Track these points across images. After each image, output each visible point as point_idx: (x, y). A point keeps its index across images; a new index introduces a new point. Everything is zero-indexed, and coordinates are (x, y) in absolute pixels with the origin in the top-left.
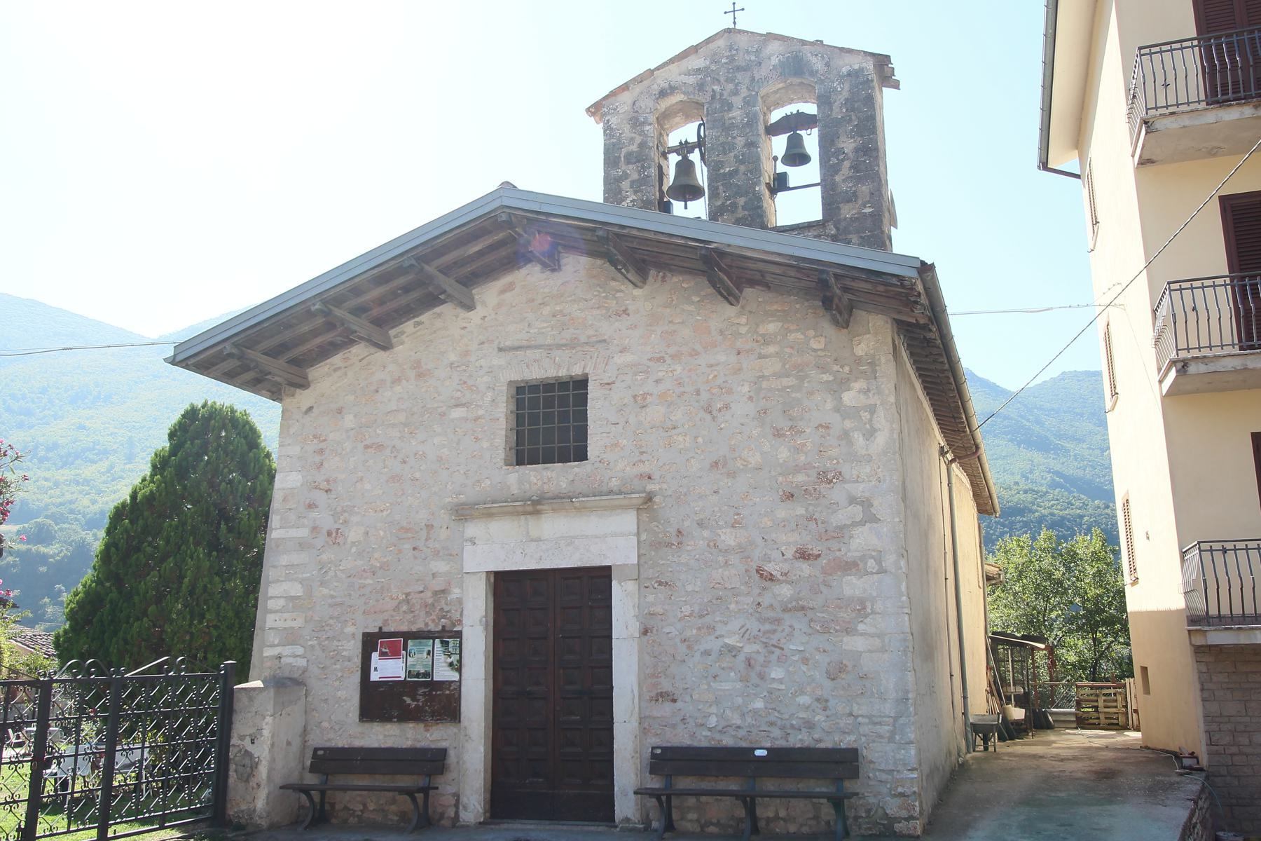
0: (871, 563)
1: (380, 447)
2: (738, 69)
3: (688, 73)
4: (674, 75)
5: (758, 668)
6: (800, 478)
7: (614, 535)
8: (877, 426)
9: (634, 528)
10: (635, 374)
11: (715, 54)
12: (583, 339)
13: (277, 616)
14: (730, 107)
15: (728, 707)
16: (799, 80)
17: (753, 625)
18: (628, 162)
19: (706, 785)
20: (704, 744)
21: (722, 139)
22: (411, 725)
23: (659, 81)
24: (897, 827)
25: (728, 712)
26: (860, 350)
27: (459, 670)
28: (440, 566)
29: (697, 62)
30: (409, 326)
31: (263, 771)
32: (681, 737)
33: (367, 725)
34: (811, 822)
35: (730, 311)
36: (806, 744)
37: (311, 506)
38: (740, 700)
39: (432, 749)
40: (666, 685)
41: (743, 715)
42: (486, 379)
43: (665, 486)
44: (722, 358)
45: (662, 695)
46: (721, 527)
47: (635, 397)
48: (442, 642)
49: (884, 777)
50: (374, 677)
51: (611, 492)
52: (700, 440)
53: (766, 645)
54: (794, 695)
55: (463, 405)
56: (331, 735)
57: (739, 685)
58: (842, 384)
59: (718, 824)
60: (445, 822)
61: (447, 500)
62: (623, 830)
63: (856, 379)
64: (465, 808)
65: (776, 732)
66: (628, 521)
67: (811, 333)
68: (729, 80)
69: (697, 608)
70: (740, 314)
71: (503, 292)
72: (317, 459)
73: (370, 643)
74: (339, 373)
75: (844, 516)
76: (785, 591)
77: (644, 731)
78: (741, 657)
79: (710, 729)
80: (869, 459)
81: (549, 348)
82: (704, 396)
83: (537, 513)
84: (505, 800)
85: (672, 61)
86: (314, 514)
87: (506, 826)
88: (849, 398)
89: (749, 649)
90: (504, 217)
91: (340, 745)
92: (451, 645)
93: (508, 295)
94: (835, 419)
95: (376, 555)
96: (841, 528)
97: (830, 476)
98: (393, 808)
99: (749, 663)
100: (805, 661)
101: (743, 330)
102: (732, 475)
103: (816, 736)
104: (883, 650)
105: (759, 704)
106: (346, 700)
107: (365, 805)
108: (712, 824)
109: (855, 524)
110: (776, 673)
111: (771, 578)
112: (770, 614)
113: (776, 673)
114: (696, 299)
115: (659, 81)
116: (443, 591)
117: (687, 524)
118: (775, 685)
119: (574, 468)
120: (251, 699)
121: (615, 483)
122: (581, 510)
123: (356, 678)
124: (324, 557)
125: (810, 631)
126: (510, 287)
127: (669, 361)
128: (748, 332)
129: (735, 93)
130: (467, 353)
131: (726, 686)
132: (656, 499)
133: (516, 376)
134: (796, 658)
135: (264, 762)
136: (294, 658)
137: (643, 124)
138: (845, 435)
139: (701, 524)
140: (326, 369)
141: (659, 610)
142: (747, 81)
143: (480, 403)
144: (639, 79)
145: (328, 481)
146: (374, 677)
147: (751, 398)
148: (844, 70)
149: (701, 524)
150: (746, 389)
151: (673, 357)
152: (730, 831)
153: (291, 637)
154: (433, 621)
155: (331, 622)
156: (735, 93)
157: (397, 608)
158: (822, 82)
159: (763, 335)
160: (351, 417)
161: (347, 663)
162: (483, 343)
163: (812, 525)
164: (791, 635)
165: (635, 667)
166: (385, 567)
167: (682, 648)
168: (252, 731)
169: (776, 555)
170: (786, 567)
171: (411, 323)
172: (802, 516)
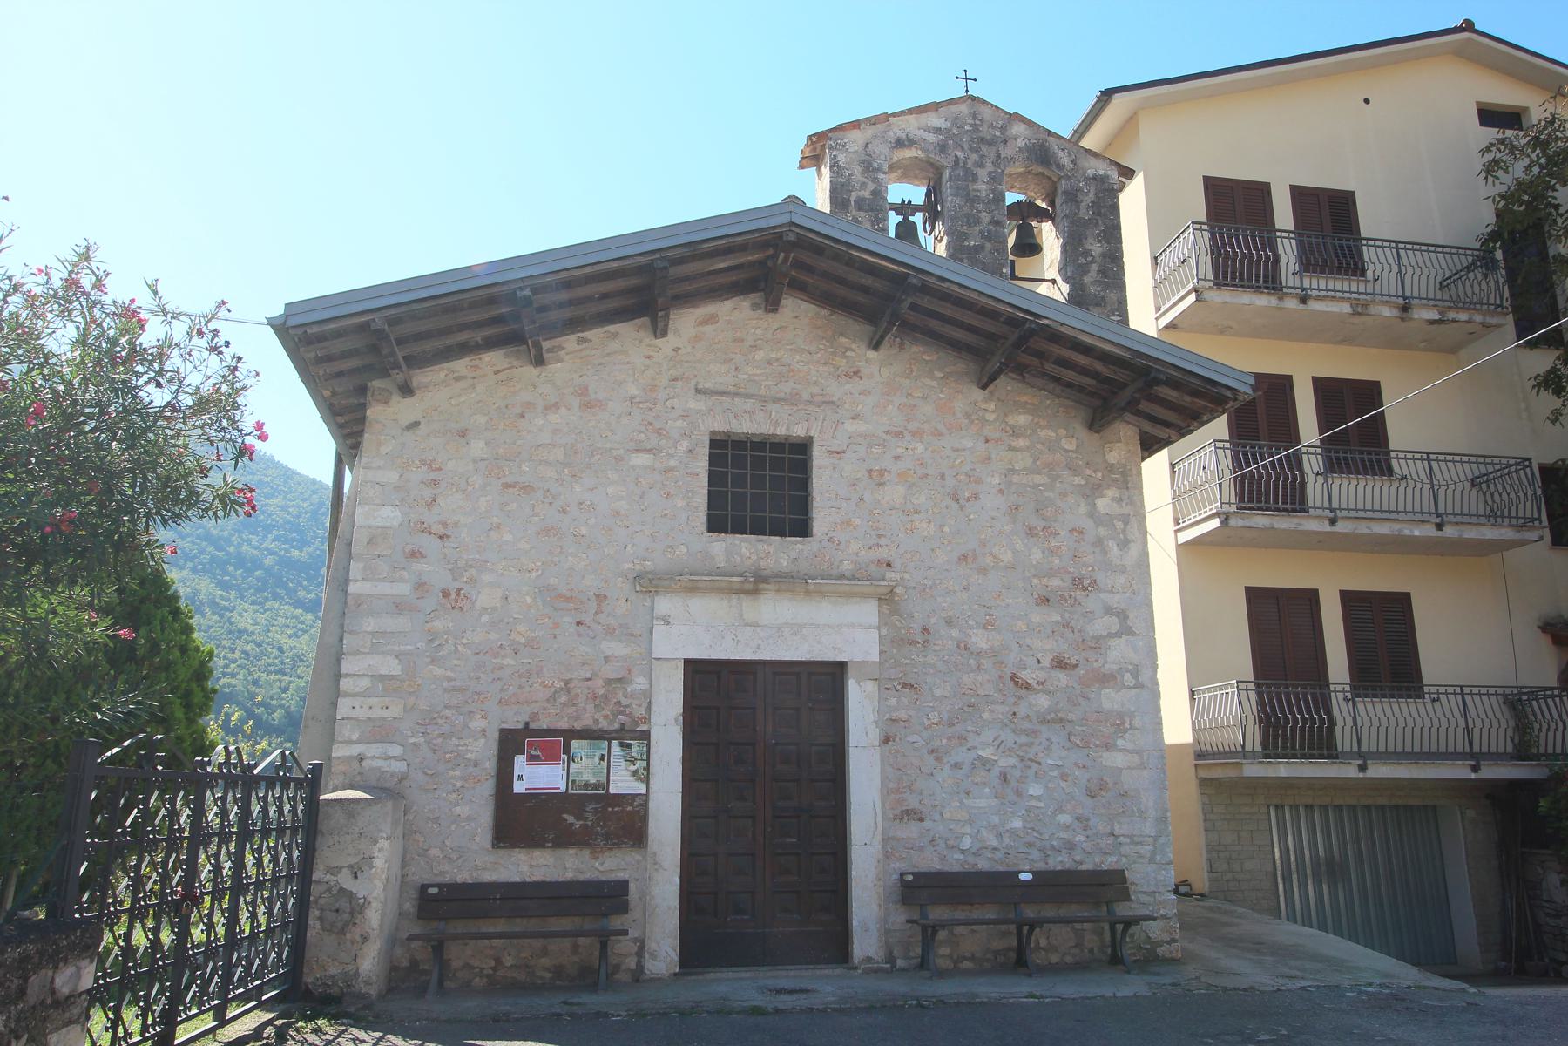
0: (1127, 676)
1: (527, 488)
2: (983, 140)
3: (928, 130)
4: (912, 125)
5: (1014, 784)
6: (1055, 582)
7: (852, 626)
8: (1130, 537)
9: (875, 620)
10: (870, 446)
11: (957, 118)
12: (806, 396)
13: (357, 702)
14: (975, 179)
15: (981, 827)
16: (1040, 170)
17: (1008, 737)
18: (860, 209)
19: (960, 914)
20: (957, 868)
21: (966, 209)
22: (571, 851)
23: (895, 129)
24: (1160, 950)
25: (984, 832)
26: (1113, 457)
27: (647, 780)
28: (617, 648)
29: (936, 121)
30: (570, 341)
31: (374, 918)
32: (930, 861)
33: (501, 852)
34: (1073, 951)
35: (978, 394)
36: (1067, 866)
37: (415, 555)
38: (996, 819)
39: (608, 882)
40: (912, 802)
41: (1000, 836)
42: (679, 423)
43: (907, 576)
44: (968, 443)
45: (907, 812)
46: (972, 628)
47: (870, 471)
48: (622, 745)
49: (1145, 898)
50: (519, 787)
51: (842, 576)
52: (946, 529)
53: (1022, 759)
54: (1054, 814)
55: (649, 451)
56: (447, 867)
57: (994, 802)
58: (1092, 491)
59: (972, 958)
60: (623, 977)
61: (627, 566)
62: (866, 972)
63: (1109, 487)
64: (654, 956)
65: (1035, 854)
66: (868, 612)
67: (1062, 432)
68: (977, 151)
69: (945, 716)
70: (986, 400)
71: (704, 322)
72: (428, 493)
73: (511, 743)
74: (462, 384)
75: (1103, 625)
76: (1042, 702)
77: (887, 855)
78: (996, 771)
79: (963, 852)
80: (1123, 570)
81: (764, 400)
82: (950, 482)
83: (755, 592)
84: (700, 947)
85: (910, 111)
86: (418, 566)
87: (712, 976)
88: (1102, 504)
89: (1005, 762)
91: (460, 879)
92: (635, 749)
93: (708, 329)
94: (1088, 524)
95: (521, 628)
96: (1098, 638)
97: (1086, 583)
98: (545, 961)
99: (1004, 778)
100: (1064, 777)
101: (991, 417)
102: (983, 571)
103: (1078, 858)
104: (1142, 766)
105: (1017, 823)
106: (469, 819)
107: (498, 961)
108: (965, 958)
109: (1110, 636)
110: (1035, 789)
111: (1027, 687)
112: (1026, 725)
113: (1035, 789)
114: (939, 374)
115: (895, 129)
116: (620, 680)
117: (933, 620)
118: (1033, 803)
119: (795, 545)
120: (351, 816)
121: (847, 567)
122: (821, 593)
123: (488, 788)
124: (438, 625)
125: (1068, 745)
126: (711, 319)
127: (908, 437)
128: (996, 420)
129: (981, 165)
130: (653, 388)
131: (981, 803)
132: (898, 590)
133: (720, 425)
134: (1055, 773)
136: (384, 758)
137: (878, 170)
138: (1099, 542)
139: (949, 622)
140: (442, 375)
141: (903, 714)
142: (992, 156)
143: (672, 451)
144: (873, 121)
145: (444, 524)
146: (519, 787)
147: (1001, 491)
148: (1090, 172)
149: (949, 622)
150: (996, 480)
151: (913, 434)
152: (987, 965)
153: (380, 731)
154: (606, 717)
155: (447, 713)
156: (981, 165)
157: (553, 698)
158: (1069, 178)
159: (1013, 427)
160: (481, 444)
161: (471, 769)
162: (675, 380)
163: (1069, 634)
164: (1048, 748)
165: (877, 781)
166: (532, 644)
167: (930, 760)
169: (1031, 661)
170: (1042, 675)
171: (573, 337)
172: (1057, 622)
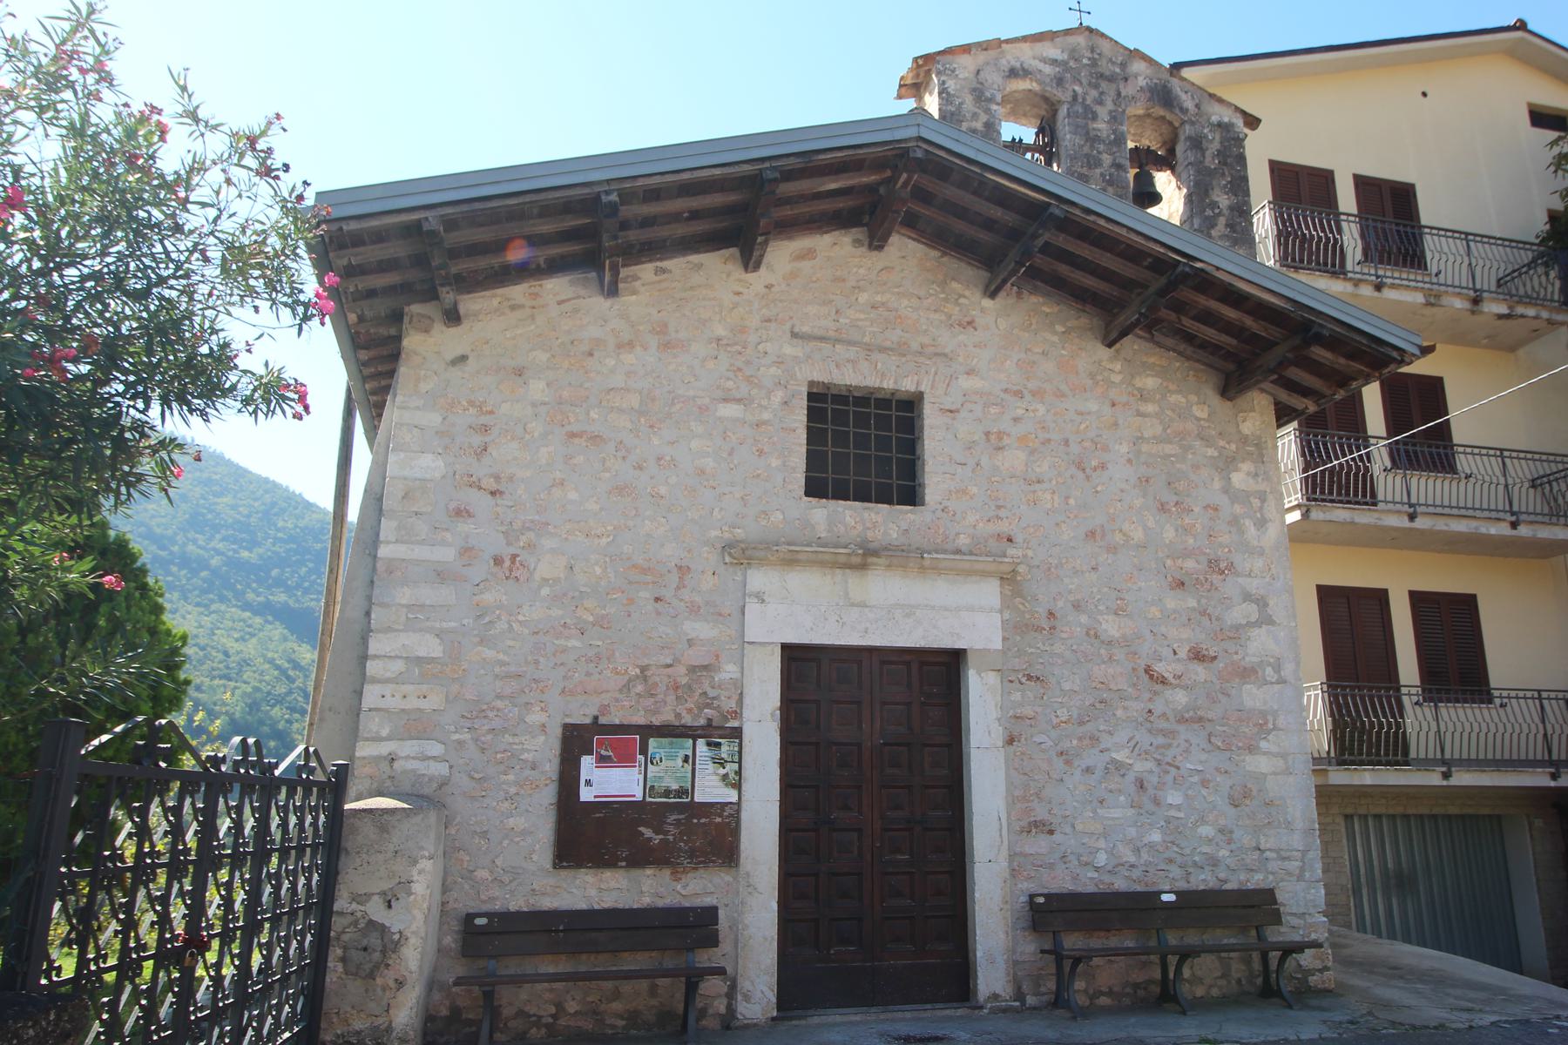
0: (1269, 670)
1: (596, 439)
3: (1044, 60)
4: (1026, 55)
5: (1151, 791)
6: (1190, 564)
7: (971, 609)
10: (986, 406)
12: (915, 346)
13: (388, 689)
14: (1095, 117)
17: (1144, 739)
19: (1096, 942)
20: (1091, 889)
21: (1086, 149)
22: (649, 872)
23: (1009, 57)
25: (1120, 846)
26: (1247, 428)
27: (738, 786)
28: (702, 630)
32: (1061, 881)
33: (564, 873)
34: (1220, 982)
35: (1103, 353)
37: (461, 513)
40: (1041, 813)
41: (1137, 851)
42: (773, 370)
43: (1030, 553)
44: (1093, 406)
45: (1036, 824)
46: (1101, 613)
47: (987, 434)
48: (709, 744)
50: (586, 795)
51: (958, 551)
52: (1072, 501)
54: (1195, 825)
55: (739, 401)
57: (1131, 812)
58: (1227, 464)
60: (710, 1023)
61: (714, 533)
62: (994, 1011)
64: (747, 998)
65: (1176, 872)
66: (989, 593)
67: (1193, 398)
68: (1096, 87)
69: (1075, 713)
70: (1111, 360)
72: (477, 440)
73: (576, 741)
74: (518, 314)
75: (1241, 613)
76: (1180, 698)
77: (1014, 873)
78: (1131, 776)
79: (1097, 869)
81: (869, 348)
82: (1074, 448)
83: (863, 567)
85: (1025, 39)
86: (464, 527)
87: (816, 1020)
88: (1239, 479)
89: (1140, 766)
90: (919, 154)
91: (513, 907)
92: (724, 748)
93: (806, 265)
94: (1223, 501)
95: (589, 603)
96: (1238, 627)
97: (1223, 565)
98: (617, 1006)
99: (1141, 785)
100: (1205, 783)
101: (1117, 378)
102: (1112, 549)
103: (1222, 875)
104: (1288, 772)
105: (1156, 837)
106: (524, 833)
107: (559, 1006)
108: (1103, 994)
109: (1250, 625)
110: (1174, 797)
112: (1163, 725)
113: (1174, 797)
114: (1059, 328)
115: (1009, 57)
116: (705, 667)
117: (1060, 604)
118: (1173, 813)
120: (384, 829)
121: (963, 541)
122: (938, 570)
123: (547, 795)
124: (488, 597)
126: (809, 254)
127: (1028, 397)
128: (1122, 382)
129: (1100, 103)
130: (743, 330)
132: (1021, 569)
134: (1195, 779)
135: (412, 940)
136: (422, 758)
137: (991, 100)
138: (1235, 521)
139: (1077, 606)
140: (495, 302)
141: (1028, 711)
142: (1113, 93)
143: (765, 402)
144: (985, 46)
145: (497, 478)
146: (586, 795)
147: (1129, 461)
148: (1214, 119)
149: (1077, 606)
150: (1124, 449)
151: (1034, 394)
152: (1126, 1001)
153: (415, 726)
154: (690, 711)
155: (499, 704)
156: (1100, 103)
157: (627, 687)
158: (1193, 123)
160: (542, 385)
161: (527, 772)
162: (769, 320)
163: (1205, 621)
164: (1187, 751)
165: (1002, 788)
167: (1059, 763)
168: (385, 886)
169: (1167, 652)
170: (1179, 668)
172: (1194, 609)
